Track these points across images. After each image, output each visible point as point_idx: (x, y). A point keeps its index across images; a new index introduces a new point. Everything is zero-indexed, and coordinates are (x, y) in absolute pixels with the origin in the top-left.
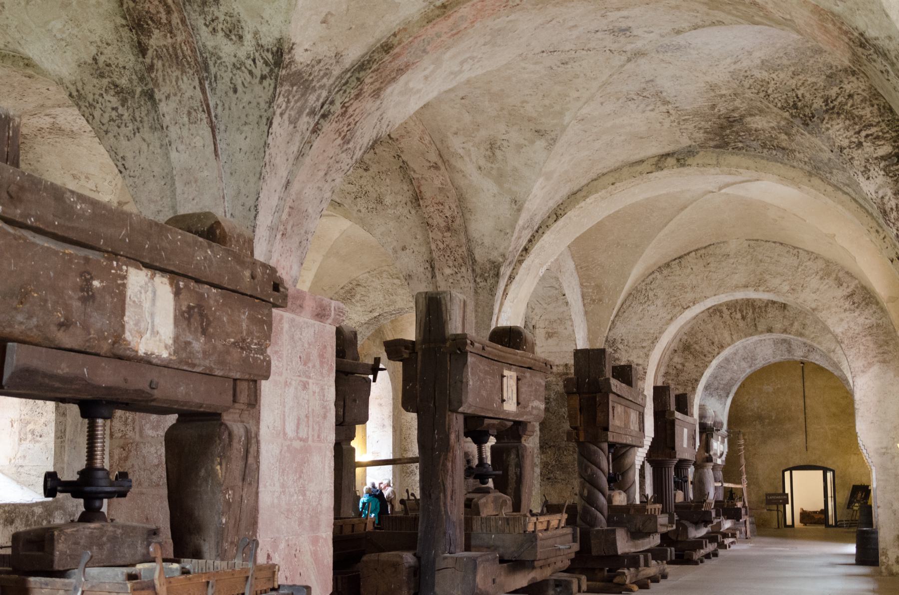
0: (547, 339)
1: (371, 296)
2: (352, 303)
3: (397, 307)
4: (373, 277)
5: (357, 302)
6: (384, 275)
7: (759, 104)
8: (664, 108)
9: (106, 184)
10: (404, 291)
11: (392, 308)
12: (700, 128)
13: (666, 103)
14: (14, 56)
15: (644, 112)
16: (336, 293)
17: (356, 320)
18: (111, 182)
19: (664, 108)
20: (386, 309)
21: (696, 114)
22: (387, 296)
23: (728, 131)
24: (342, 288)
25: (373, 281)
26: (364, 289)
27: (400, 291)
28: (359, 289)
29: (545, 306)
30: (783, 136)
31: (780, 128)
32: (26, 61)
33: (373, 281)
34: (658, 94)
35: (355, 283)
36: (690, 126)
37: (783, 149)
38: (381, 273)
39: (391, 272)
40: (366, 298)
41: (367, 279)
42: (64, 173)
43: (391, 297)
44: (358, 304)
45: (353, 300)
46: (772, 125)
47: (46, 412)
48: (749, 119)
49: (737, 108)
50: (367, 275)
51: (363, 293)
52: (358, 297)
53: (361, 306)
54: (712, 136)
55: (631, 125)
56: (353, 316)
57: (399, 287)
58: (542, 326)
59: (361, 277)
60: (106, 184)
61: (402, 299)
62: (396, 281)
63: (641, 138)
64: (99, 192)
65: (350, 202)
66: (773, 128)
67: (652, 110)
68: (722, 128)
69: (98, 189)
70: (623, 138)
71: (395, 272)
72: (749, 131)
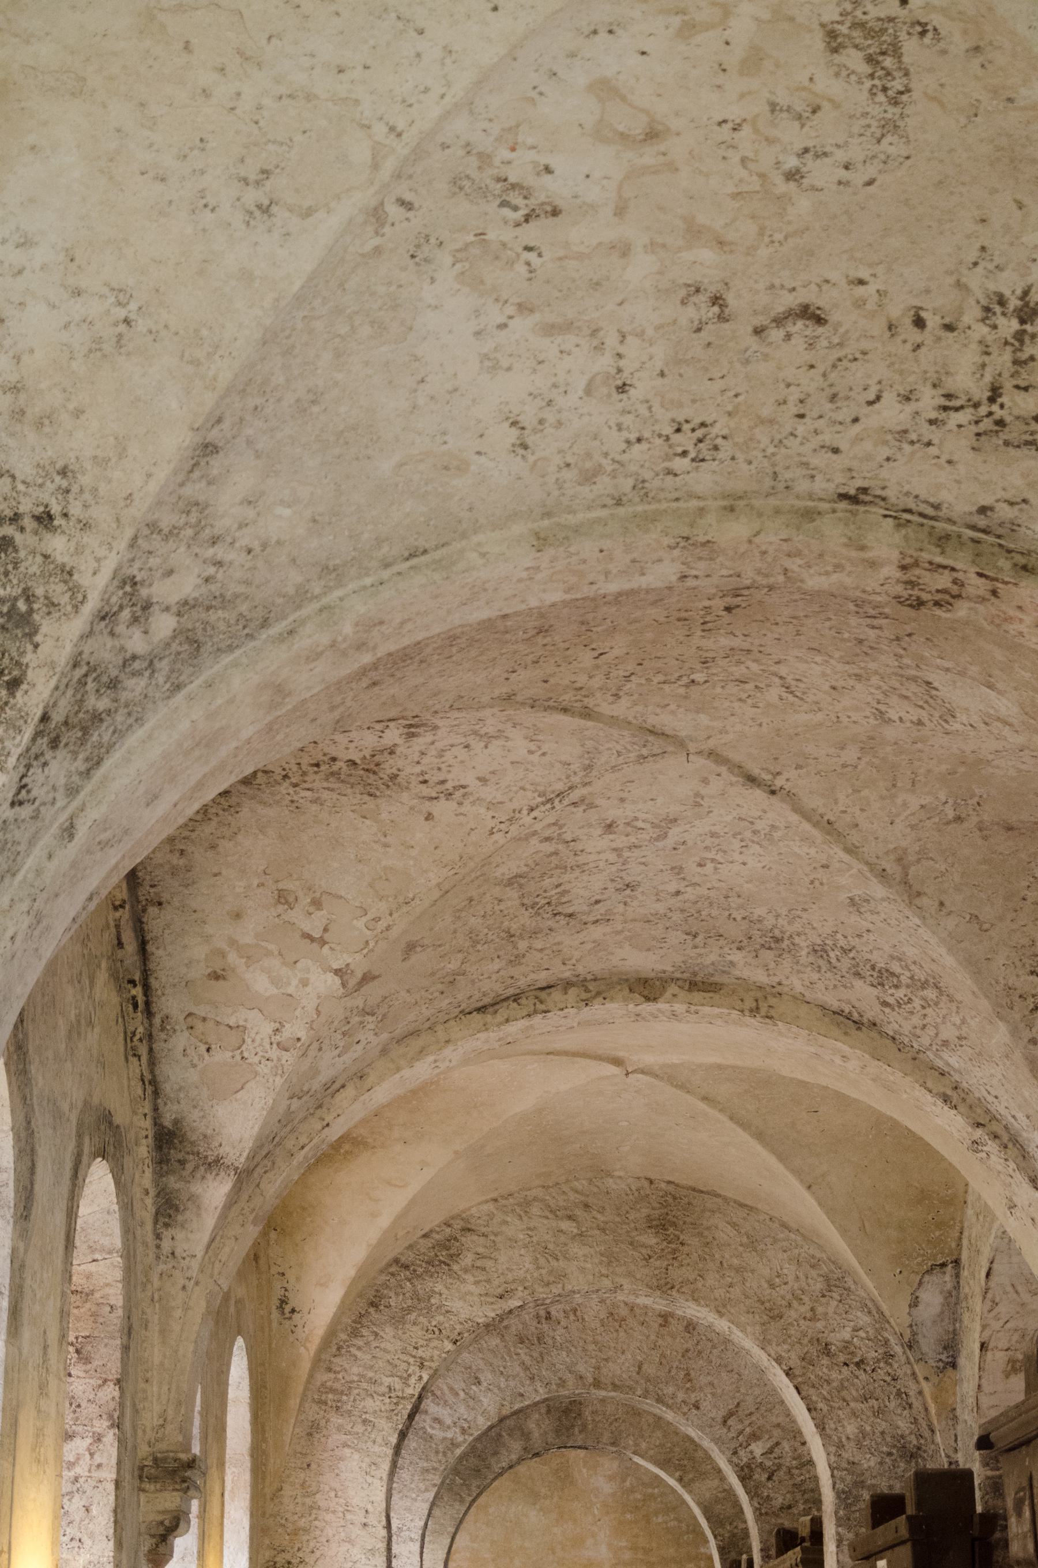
0: (1007, 1377)
1: (502, 1259)
2: (451, 1272)
3: (569, 1287)
4: (506, 1213)
5: (466, 1271)
6: (535, 1210)
9: (360, 923)
10: (586, 1250)
11: (556, 1290)
14: (974, 541)
16: (410, 1247)
17: (463, 1316)
18: (377, 919)
20: (541, 1292)
22: (542, 1261)
24: (425, 1236)
25: (505, 1222)
26: (482, 1240)
27: (576, 1249)
28: (468, 1240)
29: (1026, 1297)
32: (1021, 560)
33: (505, 1222)
35: (458, 1225)
38: (527, 1204)
39: (552, 1202)
40: (489, 1264)
41: (491, 1216)
42: (261, 885)
43: (554, 1263)
44: (470, 1278)
45: (455, 1267)
47: (92, 1535)
50: (491, 1207)
51: (481, 1250)
52: (468, 1259)
53: (476, 1283)
56: (456, 1305)
57: (573, 1238)
58: (1003, 1344)
59: (474, 1211)
60: (360, 923)
61: (582, 1270)
62: (566, 1225)
64: (323, 942)
65: (1017, 1016)
69: (326, 936)
71: (561, 1203)
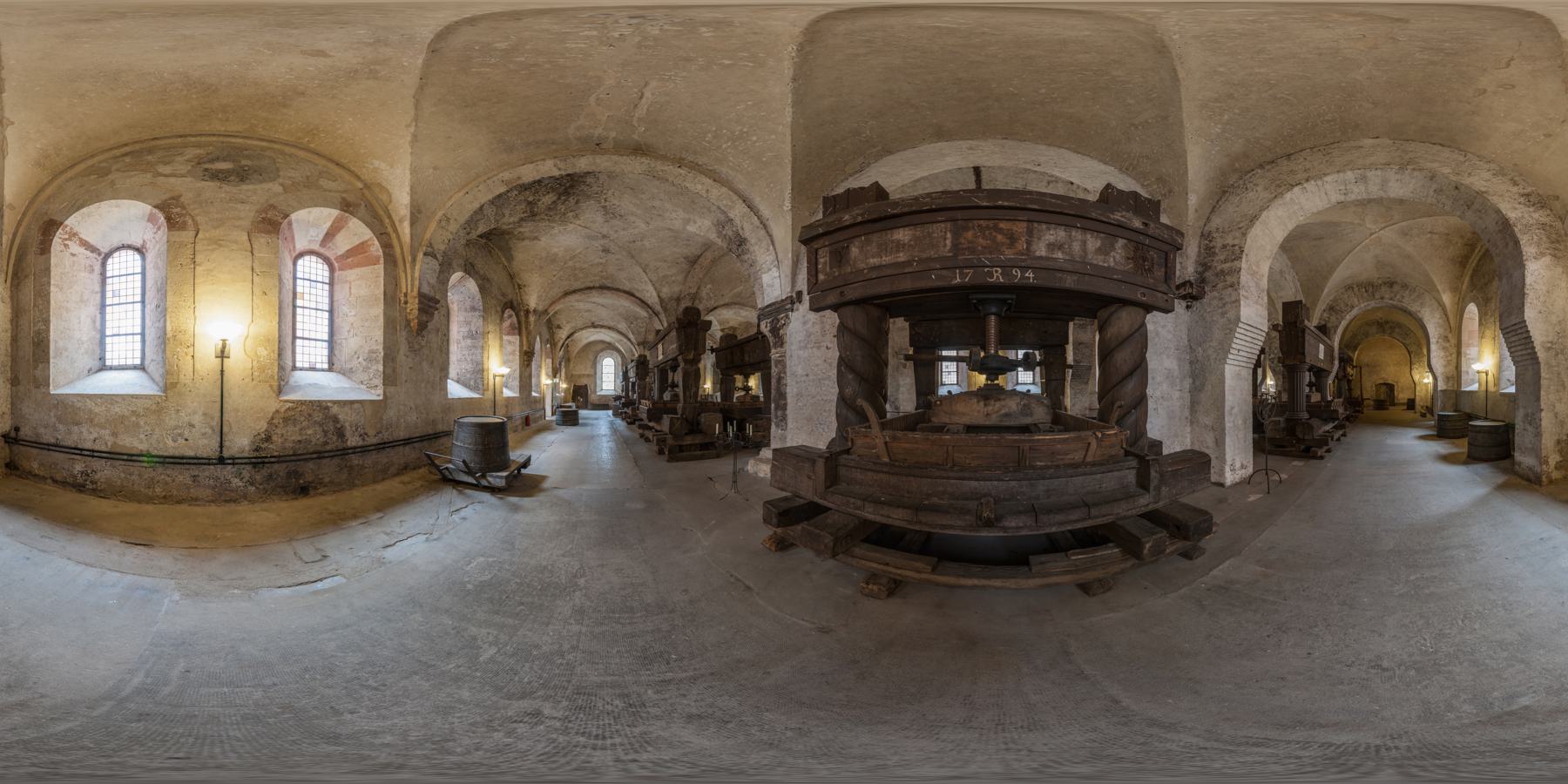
7: (552, 213)
8: (607, 204)
12: (588, 185)
13: (604, 207)
15: (619, 206)
19: (607, 204)
21: (589, 197)
23: (568, 185)
30: (531, 199)
31: (536, 203)
34: (607, 213)
36: (595, 188)
37: (526, 189)
46: (541, 202)
48: (555, 198)
49: (563, 204)
54: (581, 179)
55: (631, 202)
63: (632, 189)
66: (539, 200)
67: (614, 205)
68: (572, 187)
70: (643, 196)
72: (553, 189)
